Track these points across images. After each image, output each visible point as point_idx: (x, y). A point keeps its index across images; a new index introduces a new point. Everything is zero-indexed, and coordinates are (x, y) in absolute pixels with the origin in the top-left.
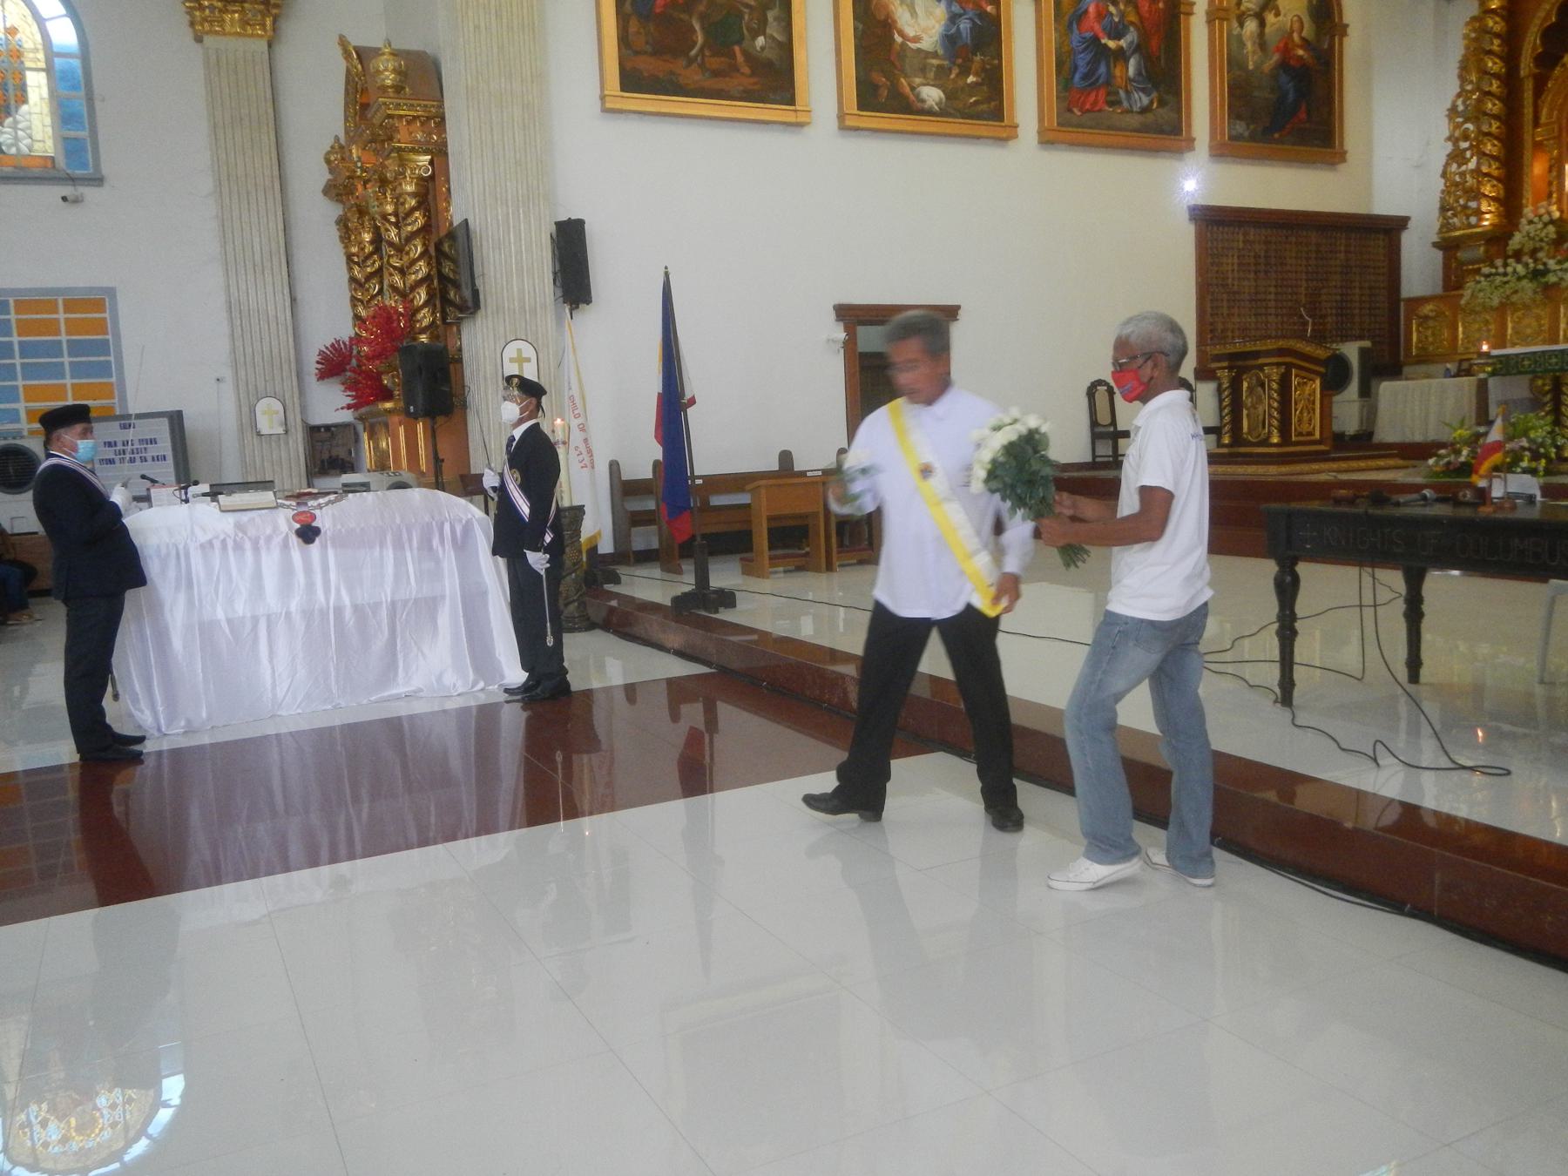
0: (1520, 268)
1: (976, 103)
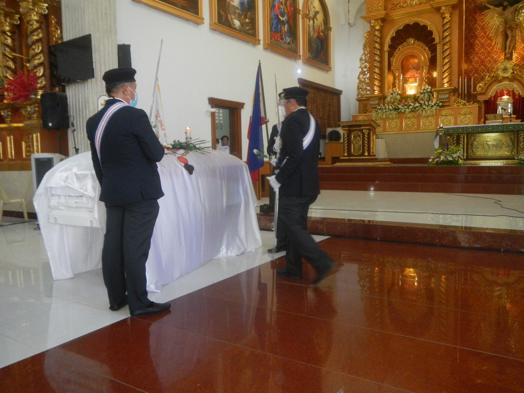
0: (390, 107)
1: (248, 30)
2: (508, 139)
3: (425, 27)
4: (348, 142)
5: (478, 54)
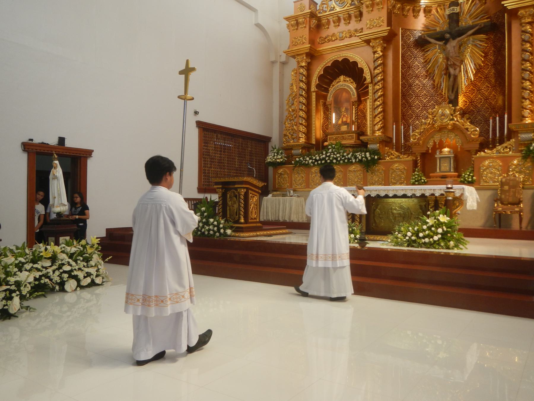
2: (418, 207)
3: (355, 63)
4: (222, 204)
5: (419, 96)
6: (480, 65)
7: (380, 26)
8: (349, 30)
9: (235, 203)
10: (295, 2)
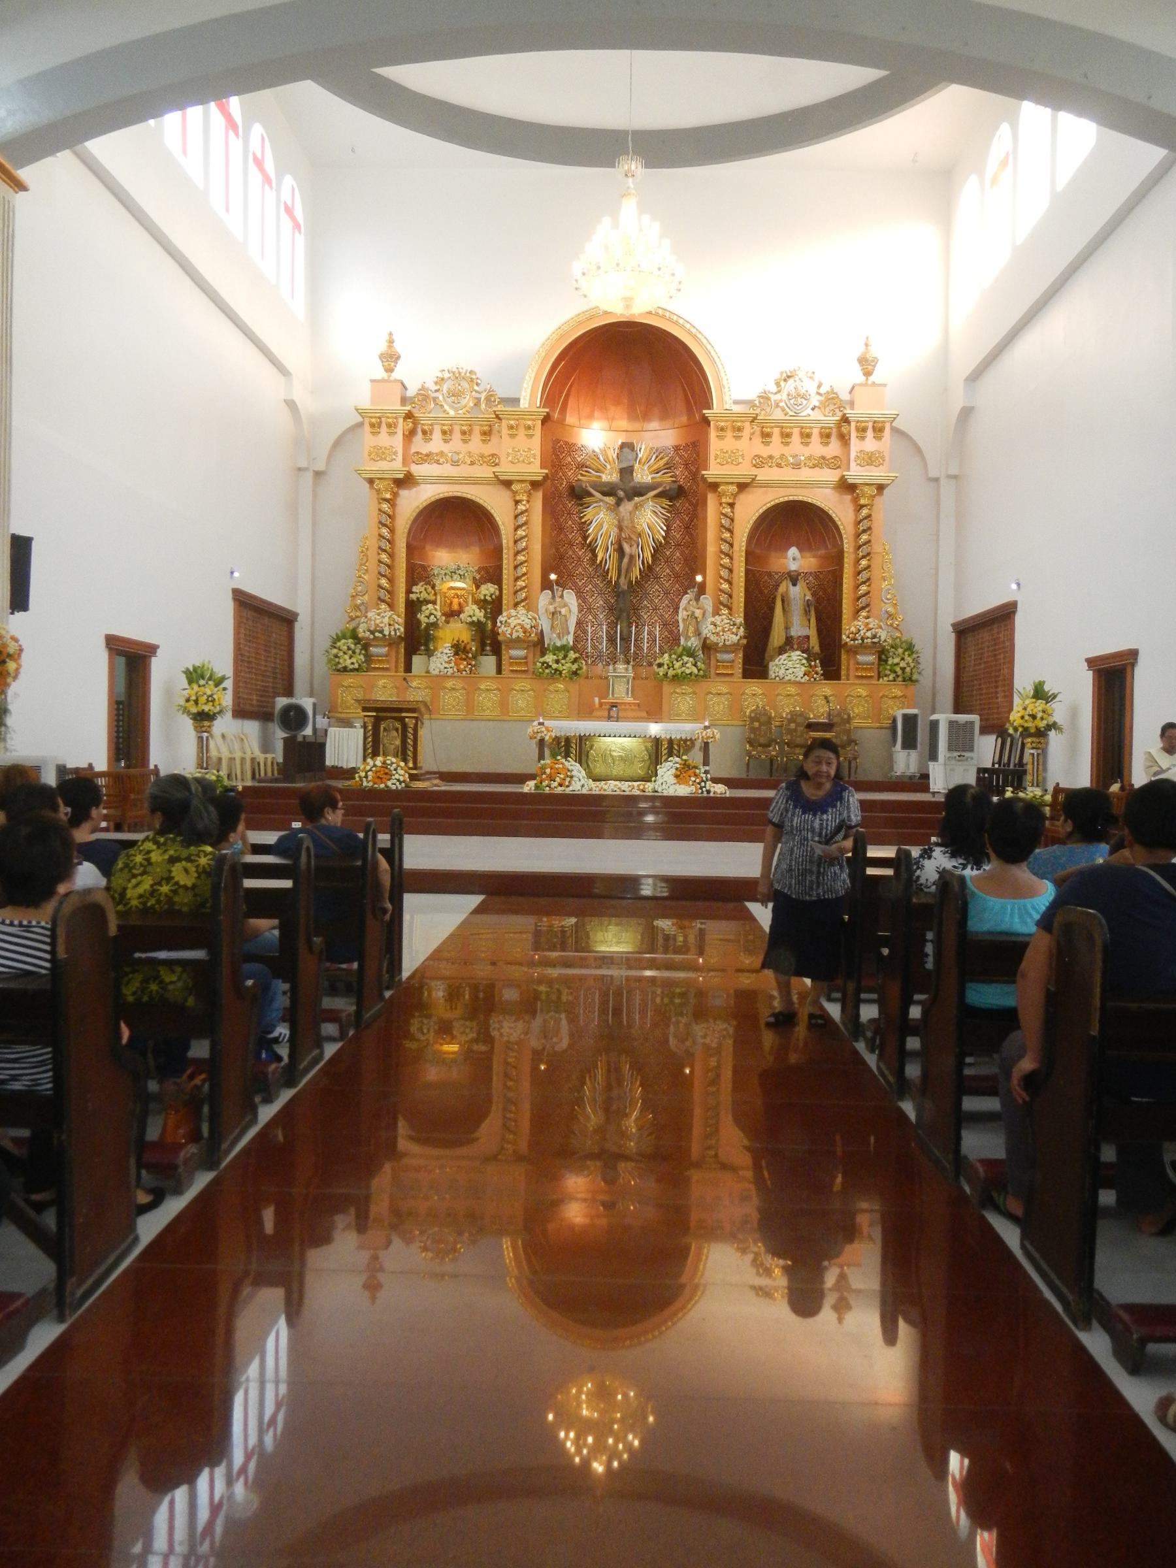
6: (661, 543)
7: (530, 463)
8: (470, 452)
9: (396, 739)
10: (372, 381)
